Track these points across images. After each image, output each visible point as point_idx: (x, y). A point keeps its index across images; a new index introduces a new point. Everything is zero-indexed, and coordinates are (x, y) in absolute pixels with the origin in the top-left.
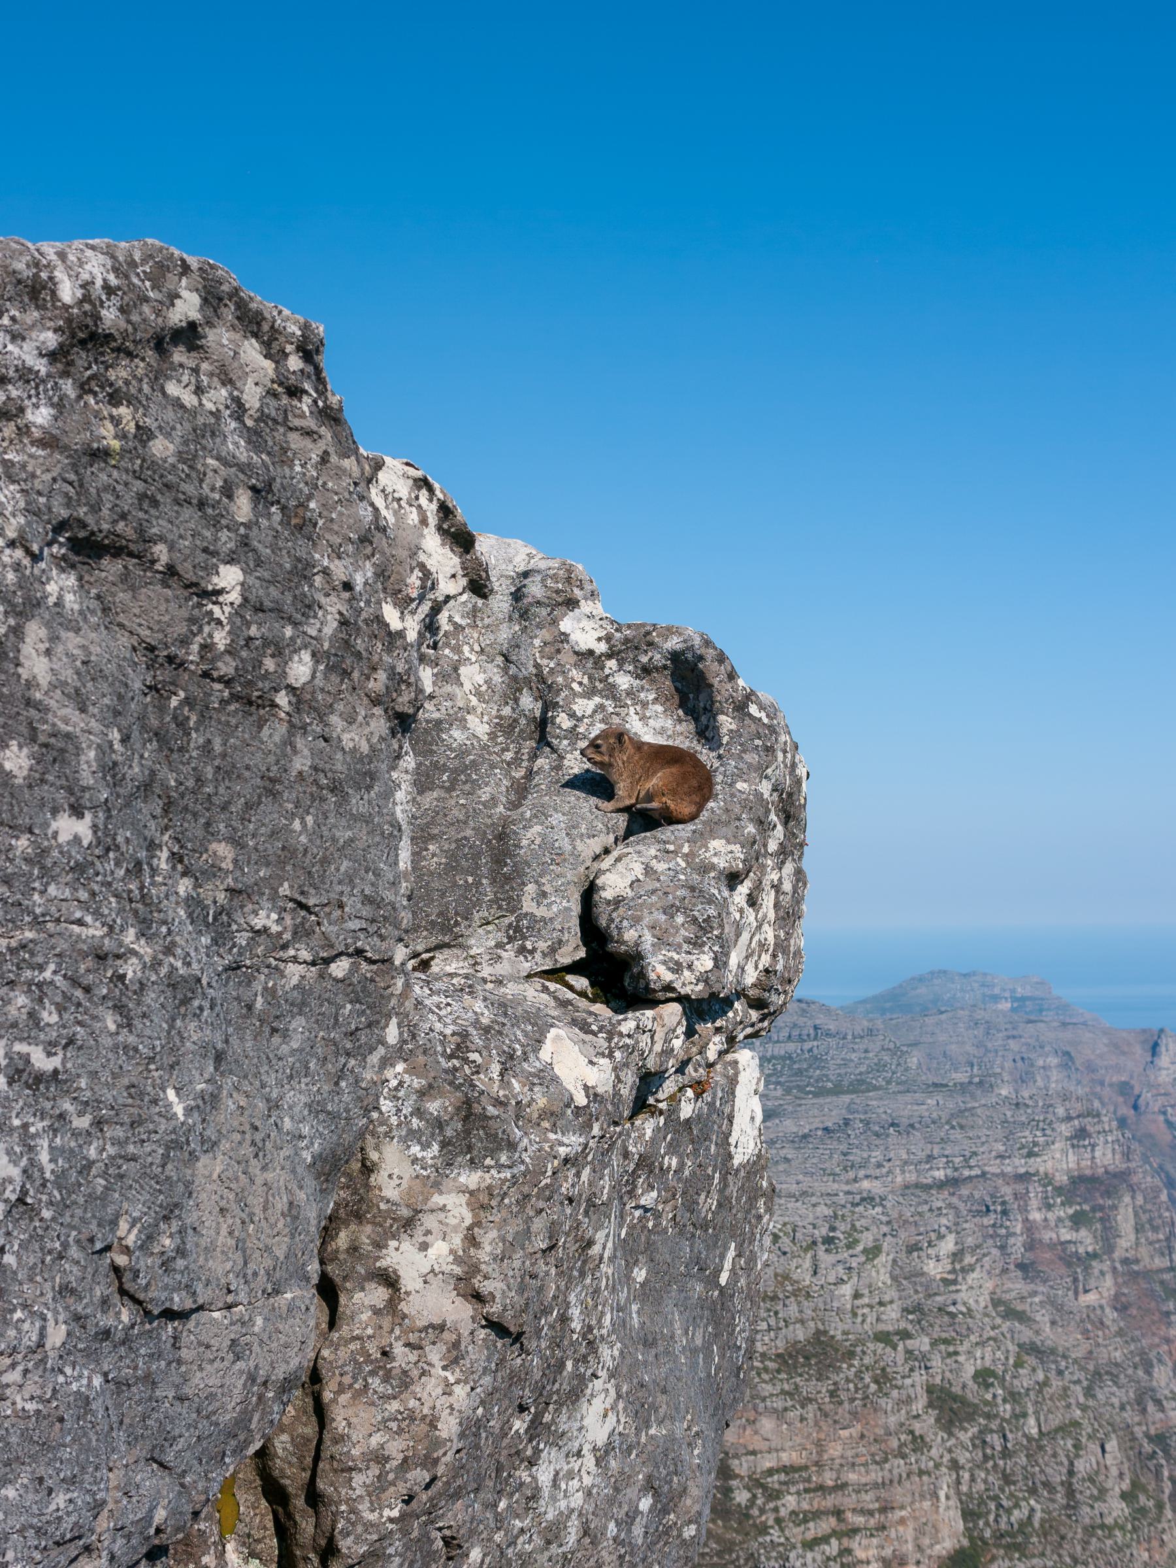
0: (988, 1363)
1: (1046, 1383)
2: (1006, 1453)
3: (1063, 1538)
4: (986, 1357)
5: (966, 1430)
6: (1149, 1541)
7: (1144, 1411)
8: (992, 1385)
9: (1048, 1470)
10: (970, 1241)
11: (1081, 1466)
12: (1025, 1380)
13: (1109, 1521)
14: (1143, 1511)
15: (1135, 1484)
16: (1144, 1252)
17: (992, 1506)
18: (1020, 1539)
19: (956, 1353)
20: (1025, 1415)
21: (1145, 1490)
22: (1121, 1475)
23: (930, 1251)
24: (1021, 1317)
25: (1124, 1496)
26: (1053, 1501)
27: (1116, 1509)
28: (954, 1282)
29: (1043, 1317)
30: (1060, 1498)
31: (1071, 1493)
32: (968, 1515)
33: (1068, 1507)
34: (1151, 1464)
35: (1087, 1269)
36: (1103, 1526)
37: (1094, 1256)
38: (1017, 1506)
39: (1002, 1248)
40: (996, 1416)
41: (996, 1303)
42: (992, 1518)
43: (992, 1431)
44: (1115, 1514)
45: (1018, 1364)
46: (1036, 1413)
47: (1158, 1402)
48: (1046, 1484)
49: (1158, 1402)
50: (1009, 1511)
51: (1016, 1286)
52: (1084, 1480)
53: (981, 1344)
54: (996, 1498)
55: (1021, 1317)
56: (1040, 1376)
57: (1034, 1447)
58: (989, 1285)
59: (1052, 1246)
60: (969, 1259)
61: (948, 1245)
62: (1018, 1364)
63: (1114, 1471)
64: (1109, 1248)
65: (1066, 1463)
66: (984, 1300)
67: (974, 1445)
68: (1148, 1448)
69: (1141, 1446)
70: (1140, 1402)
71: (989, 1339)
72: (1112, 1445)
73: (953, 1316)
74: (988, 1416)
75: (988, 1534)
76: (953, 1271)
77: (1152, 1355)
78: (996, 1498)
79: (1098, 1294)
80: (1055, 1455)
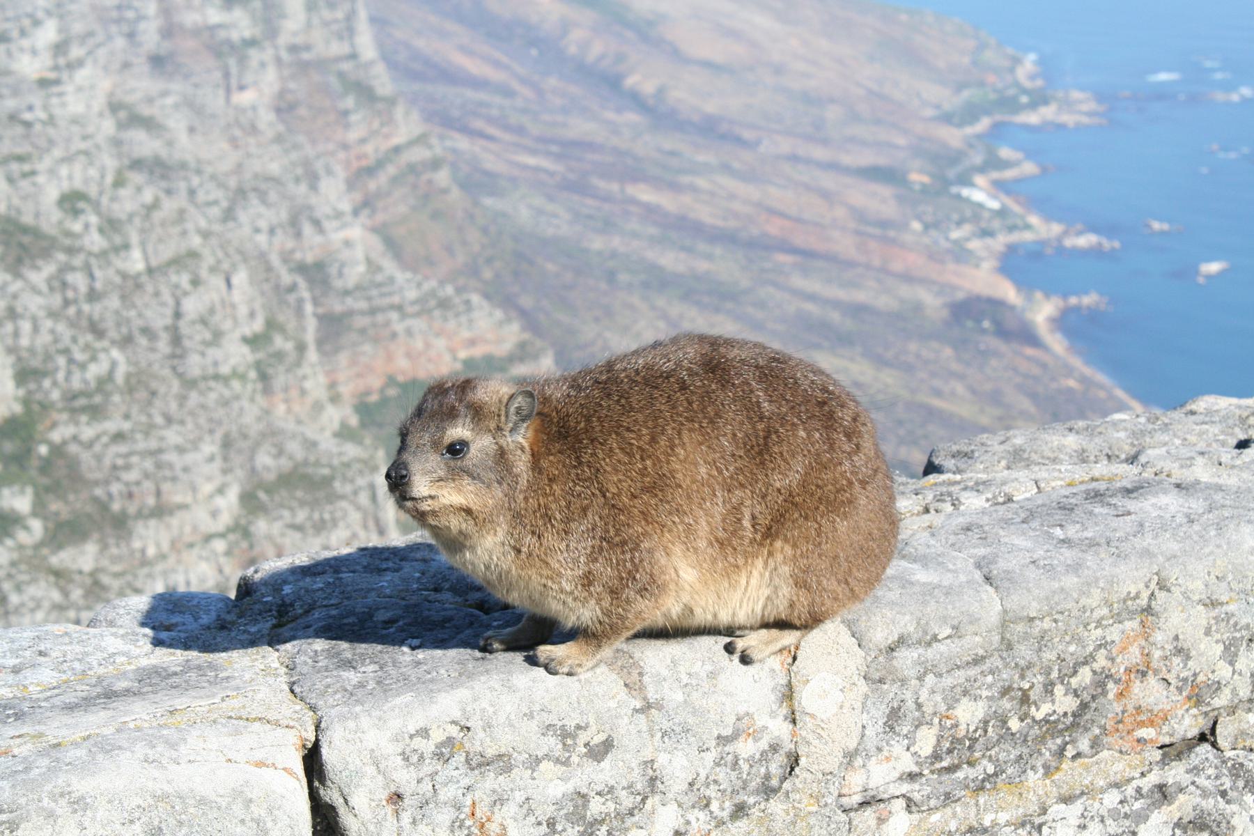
0: (78, 184)
1: (155, 205)
2: (93, 296)
3: (154, 393)
4: (76, 176)
5: (38, 269)
6: (286, 389)
7: (298, 235)
8: (82, 211)
9: (149, 313)
10: (78, 28)
11: (191, 306)
12: (126, 203)
13: (225, 370)
14: (279, 356)
15: (271, 324)
16: (317, 36)
17: (61, 361)
18: (98, 399)
19: (33, 173)
20: (126, 246)
21: (282, 329)
22: (252, 315)
23: (25, 43)
24: (149, 124)
25: (253, 341)
26: (153, 350)
27: (235, 354)
28: (57, 82)
29: (177, 124)
30: (163, 346)
31: (176, 339)
32: (24, 375)
33: (173, 356)
34: (291, 298)
35: (243, 60)
36: (216, 377)
37: (252, 43)
38: (94, 359)
39: (131, 36)
40: (80, 250)
41: (114, 107)
42: (60, 376)
43: (73, 269)
44: (233, 361)
45: (119, 183)
46: (143, 244)
47: (317, 223)
48: (146, 331)
49: (317, 223)
50: (83, 367)
51: (141, 85)
52: (193, 323)
53: (68, 159)
54: (66, 351)
55: (149, 124)
56: (148, 196)
57: (131, 286)
58: (105, 84)
59: (196, 32)
60: (76, 52)
61: (48, 33)
62: (119, 183)
63: (243, 310)
64: (272, 32)
65: (170, 301)
66: (99, 103)
67: (51, 289)
68: (287, 278)
69: (278, 277)
70: (294, 223)
71: (80, 152)
72: (240, 278)
73: (28, 125)
74: (70, 251)
75: (55, 395)
76: (56, 68)
77: (319, 166)
78: (66, 351)
79: (258, 93)
80: (157, 294)
